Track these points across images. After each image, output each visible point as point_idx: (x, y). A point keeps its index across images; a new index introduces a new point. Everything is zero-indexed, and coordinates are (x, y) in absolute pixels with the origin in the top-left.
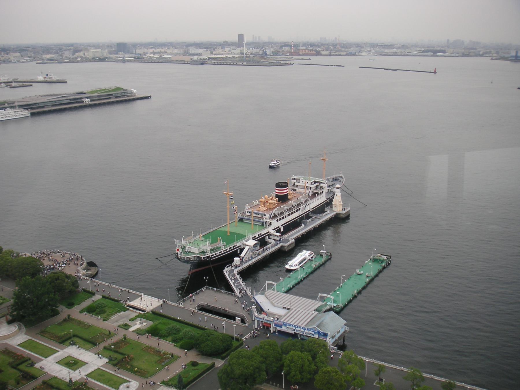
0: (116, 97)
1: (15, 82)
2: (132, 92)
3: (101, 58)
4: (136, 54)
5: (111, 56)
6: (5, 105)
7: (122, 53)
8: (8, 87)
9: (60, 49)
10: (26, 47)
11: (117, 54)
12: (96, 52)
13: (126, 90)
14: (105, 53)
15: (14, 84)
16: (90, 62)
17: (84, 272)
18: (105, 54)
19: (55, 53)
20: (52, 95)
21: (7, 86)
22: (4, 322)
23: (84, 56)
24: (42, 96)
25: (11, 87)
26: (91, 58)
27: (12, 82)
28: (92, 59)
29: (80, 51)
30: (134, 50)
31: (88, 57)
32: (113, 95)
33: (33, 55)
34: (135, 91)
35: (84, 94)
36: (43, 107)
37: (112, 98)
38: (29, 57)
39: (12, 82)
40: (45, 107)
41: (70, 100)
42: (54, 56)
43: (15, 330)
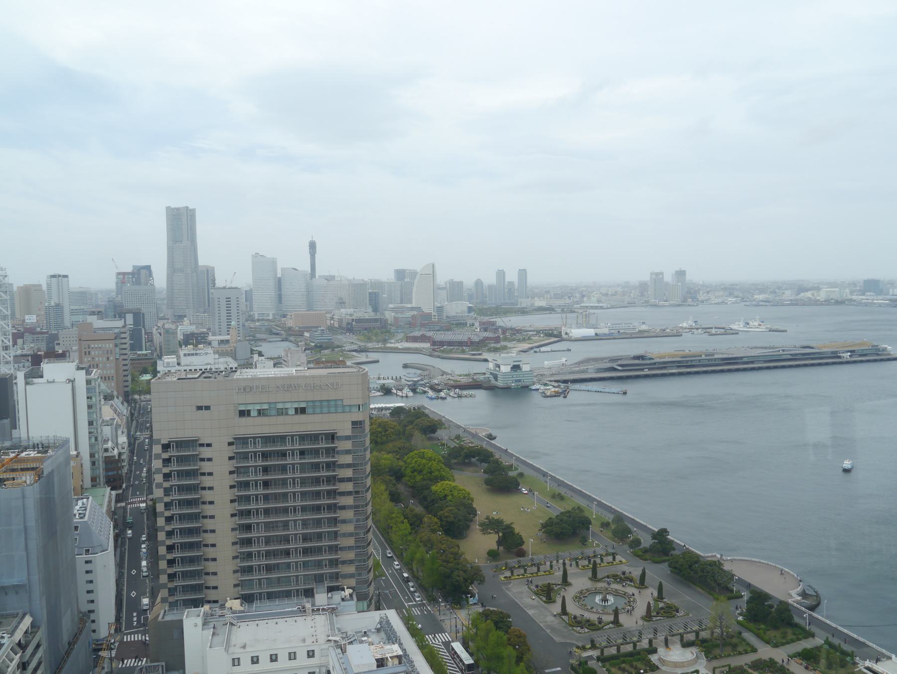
0: (861, 355)
1: (715, 328)
2: (885, 350)
3: (839, 300)
4: (893, 295)
5: (854, 297)
6: (701, 356)
7: (871, 293)
8: (707, 334)
9: (779, 288)
10: (732, 285)
11: (863, 294)
12: (831, 292)
13: (877, 346)
14: (847, 294)
15: (713, 331)
16: (822, 304)
17: (799, 598)
18: (845, 294)
19: (771, 292)
20: (765, 348)
21: (705, 333)
22: (677, 643)
23: (813, 298)
24: (751, 348)
25: (710, 334)
26: (823, 300)
27: (712, 328)
28: (825, 301)
29: (807, 290)
30: (891, 290)
31: (818, 298)
32: (856, 351)
33: (741, 295)
34: (890, 347)
35: (813, 348)
36: (752, 362)
37: (853, 356)
38: (736, 297)
39: (712, 328)
40: (755, 362)
41: (791, 355)
42: (770, 296)
43: (692, 658)
